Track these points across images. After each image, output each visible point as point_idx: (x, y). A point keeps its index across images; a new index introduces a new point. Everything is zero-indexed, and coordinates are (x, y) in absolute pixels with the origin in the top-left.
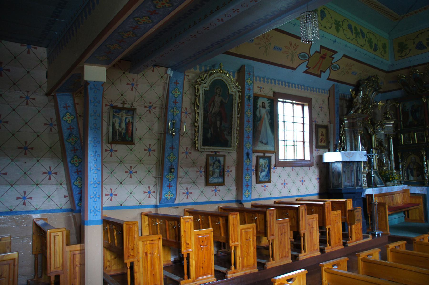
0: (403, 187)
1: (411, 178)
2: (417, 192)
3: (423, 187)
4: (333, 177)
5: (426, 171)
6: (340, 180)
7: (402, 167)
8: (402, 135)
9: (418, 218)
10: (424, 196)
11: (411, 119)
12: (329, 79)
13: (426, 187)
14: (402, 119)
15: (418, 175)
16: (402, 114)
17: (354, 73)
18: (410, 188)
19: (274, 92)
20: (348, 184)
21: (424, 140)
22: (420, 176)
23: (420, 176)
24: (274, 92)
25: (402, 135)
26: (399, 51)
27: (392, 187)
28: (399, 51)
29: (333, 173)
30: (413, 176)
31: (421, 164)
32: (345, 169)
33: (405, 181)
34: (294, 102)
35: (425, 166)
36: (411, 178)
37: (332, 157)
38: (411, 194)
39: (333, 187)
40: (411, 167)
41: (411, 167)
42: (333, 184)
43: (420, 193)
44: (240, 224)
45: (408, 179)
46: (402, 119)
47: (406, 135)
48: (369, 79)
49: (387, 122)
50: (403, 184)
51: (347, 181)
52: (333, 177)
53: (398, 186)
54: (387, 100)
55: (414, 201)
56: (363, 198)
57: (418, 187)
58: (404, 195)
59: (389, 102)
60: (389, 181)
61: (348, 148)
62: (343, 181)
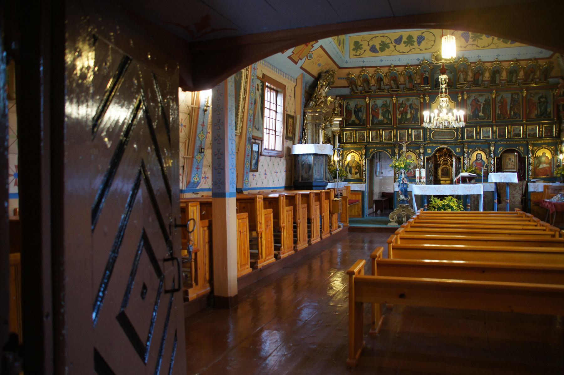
2: (356, 189)
4: (303, 169)
6: (311, 172)
9: (357, 214)
11: (353, 118)
12: (302, 68)
15: (356, 173)
17: (319, 65)
19: (263, 74)
20: (318, 177)
24: (263, 74)
26: (354, 50)
28: (354, 50)
29: (303, 165)
32: (315, 162)
34: (272, 87)
37: (299, 149)
39: (302, 180)
40: (350, 165)
42: (302, 176)
43: (359, 190)
44: (286, 206)
48: (327, 72)
50: (343, 182)
51: (317, 173)
52: (303, 169)
54: (336, 97)
55: (354, 198)
59: (338, 98)
61: (309, 141)
62: (314, 174)
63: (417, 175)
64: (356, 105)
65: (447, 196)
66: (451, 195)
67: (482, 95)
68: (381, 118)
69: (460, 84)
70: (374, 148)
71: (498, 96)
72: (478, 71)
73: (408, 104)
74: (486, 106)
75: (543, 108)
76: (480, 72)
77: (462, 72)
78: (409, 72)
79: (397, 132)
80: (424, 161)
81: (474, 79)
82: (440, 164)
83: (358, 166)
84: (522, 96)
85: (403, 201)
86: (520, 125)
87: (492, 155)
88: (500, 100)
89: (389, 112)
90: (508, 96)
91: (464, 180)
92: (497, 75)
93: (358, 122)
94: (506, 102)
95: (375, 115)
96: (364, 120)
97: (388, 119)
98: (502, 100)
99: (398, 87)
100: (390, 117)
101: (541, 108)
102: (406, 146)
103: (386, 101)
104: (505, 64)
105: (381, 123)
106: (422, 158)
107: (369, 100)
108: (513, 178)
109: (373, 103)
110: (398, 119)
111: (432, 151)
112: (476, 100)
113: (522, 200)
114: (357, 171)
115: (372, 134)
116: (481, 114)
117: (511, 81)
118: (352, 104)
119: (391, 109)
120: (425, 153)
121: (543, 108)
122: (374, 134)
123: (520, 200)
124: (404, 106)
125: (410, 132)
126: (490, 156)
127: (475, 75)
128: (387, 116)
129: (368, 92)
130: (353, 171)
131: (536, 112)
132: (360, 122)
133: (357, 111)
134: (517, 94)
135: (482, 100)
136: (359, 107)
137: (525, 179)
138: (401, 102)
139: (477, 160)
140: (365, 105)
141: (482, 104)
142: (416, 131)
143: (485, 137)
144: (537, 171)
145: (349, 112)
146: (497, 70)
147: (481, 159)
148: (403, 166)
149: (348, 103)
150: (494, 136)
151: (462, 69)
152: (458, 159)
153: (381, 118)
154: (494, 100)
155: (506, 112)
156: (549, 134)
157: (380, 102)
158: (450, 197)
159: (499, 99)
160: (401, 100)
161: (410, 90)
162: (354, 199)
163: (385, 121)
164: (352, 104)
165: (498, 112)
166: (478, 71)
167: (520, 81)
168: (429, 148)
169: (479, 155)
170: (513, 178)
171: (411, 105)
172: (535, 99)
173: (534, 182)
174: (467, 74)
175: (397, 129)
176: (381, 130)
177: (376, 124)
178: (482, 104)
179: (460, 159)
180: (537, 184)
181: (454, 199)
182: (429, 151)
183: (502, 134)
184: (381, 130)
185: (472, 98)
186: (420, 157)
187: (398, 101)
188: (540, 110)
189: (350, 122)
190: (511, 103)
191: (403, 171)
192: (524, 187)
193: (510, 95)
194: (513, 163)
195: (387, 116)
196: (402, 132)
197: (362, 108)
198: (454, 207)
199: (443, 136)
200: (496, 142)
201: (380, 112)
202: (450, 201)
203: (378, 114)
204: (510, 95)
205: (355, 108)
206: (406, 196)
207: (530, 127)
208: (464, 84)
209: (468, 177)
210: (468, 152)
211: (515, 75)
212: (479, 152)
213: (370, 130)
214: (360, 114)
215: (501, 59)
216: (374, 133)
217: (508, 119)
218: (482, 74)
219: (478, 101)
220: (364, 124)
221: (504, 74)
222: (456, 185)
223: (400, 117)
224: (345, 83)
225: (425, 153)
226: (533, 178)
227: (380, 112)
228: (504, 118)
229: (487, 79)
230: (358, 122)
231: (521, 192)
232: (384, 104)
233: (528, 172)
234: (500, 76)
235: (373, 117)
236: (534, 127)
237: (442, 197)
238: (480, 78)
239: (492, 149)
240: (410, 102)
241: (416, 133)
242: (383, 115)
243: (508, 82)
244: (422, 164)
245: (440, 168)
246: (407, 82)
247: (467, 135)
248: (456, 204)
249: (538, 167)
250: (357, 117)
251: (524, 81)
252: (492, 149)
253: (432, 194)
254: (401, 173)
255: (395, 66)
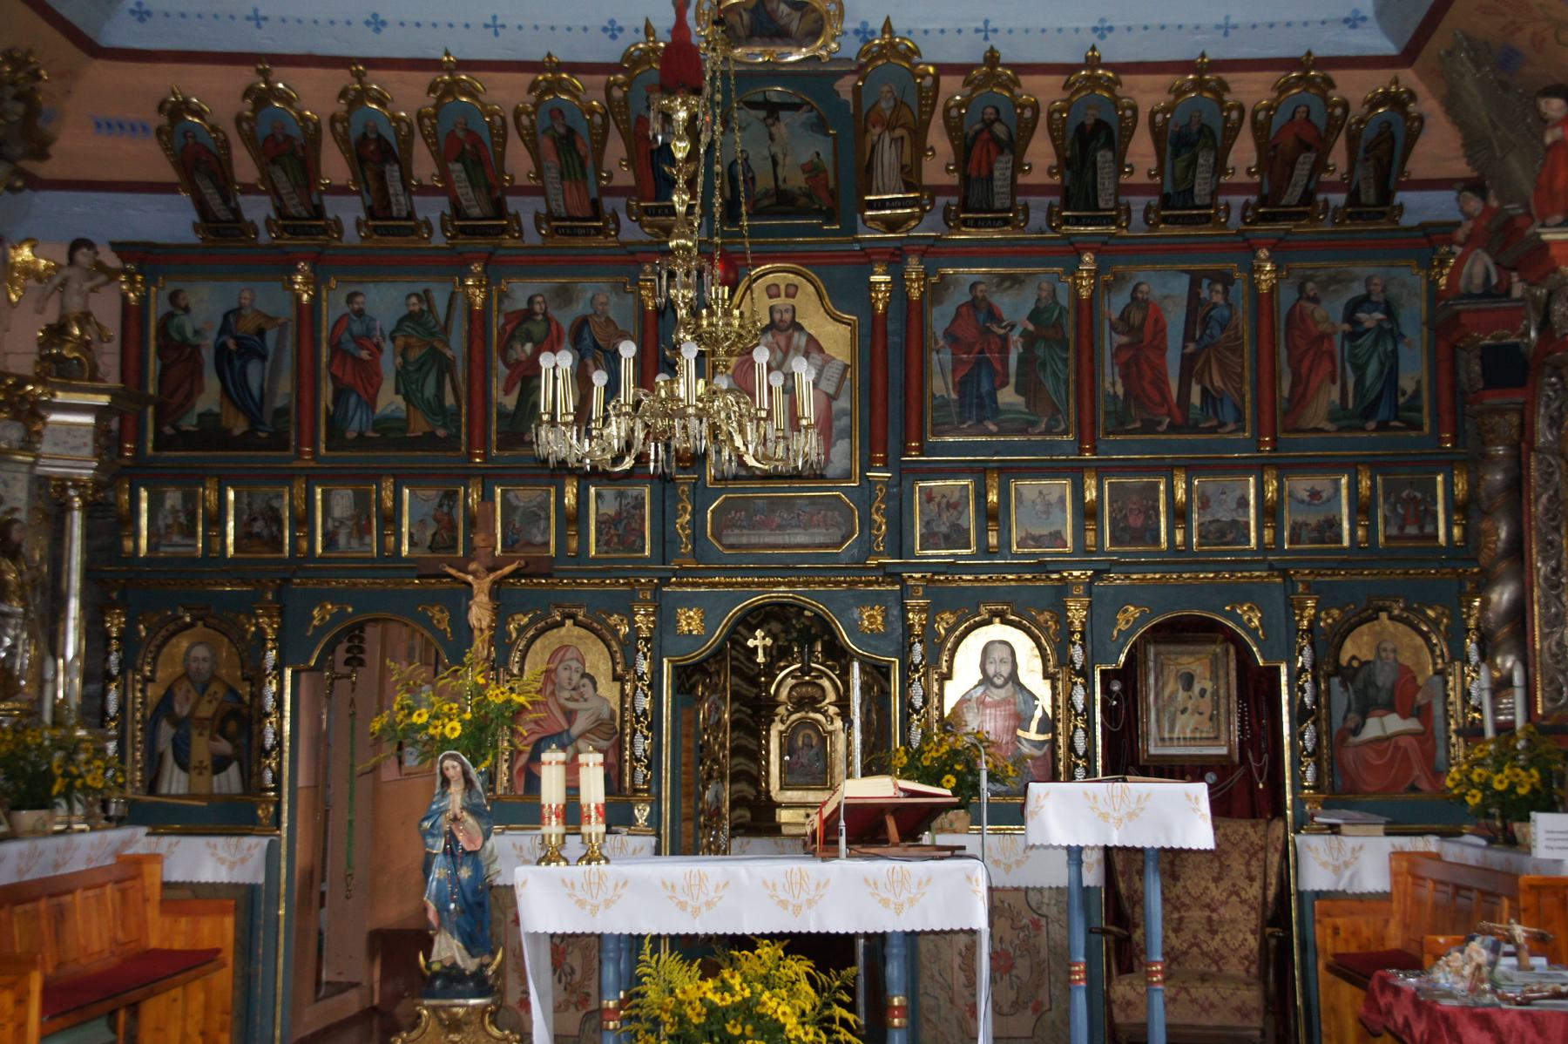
0: (126, 843)
1: (175, 782)
3: (248, 841)
5: (270, 740)
7: (122, 708)
8: (144, 494)
10: (244, 901)
11: (210, 397)
13: (265, 841)
14: (152, 390)
15: (220, 764)
16: (161, 354)
18: (164, 844)
21: (277, 543)
22: (233, 770)
23: (233, 770)
25: (144, 494)
27: (62, 840)
30: (184, 766)
31: (245, 690)
33: (131, 804)
35: (270, 704)
36: (175, 782)
38: (167, 886)
41: (181, 709)
45: (152, 786)
46: (152, 390)
47: (173, 498)
49: (61, 397)
50: (120, 822)
53: (95, 837)
56: (1221, 808)
57: (220, 841)
58: (123, 892)
60: (42, 802)
63: (552, 790)
64: (231, 318)
65: (746, 942)
66: (773, 937)
67: (1016, 281)
68: (389, 401)
69: (882, 205)
70: (333, 596)
71: (1108, 286)
72: (988, 125)
73: (565, 319)
74: (1040, 350)
75: (1372, 370)
76: (999, 130)
77: (890, 127)
78: (557, 112)
79: (487, 497)
80: (655, 686)
81: (965, 179)
82: (773, 703)
83: (233, 714)
84: (1254, 286)
85: (453, 979)
86: (1243, 468)
87: (1077, 653)
88: (1124, 316)
89: (446, 367)
90: (1169, 289)
91: (868, 830)
92: (1103, 157)
93: (239, 426)
94: (1160, 329)
95: (358, 380)
96: (282, 412)
97: (436, 409)
98: (1136, 317)
99: (499, 210)
100: (449, 400)
101: (1360, 370)
102: (495, 593)
103: (426, 297)
104: (1147, 95)
105: (390, 434)
106: (644, 666)
107: (315, 282)
108: (1182, 816)
109: (343, 308)
110: (502, 415)
111: (709, 626)
112: (980, 308)
113: (1264, 944)
114: (225, 747)
115: (331, 505)
116: (1008, 396)
117: (1185, 196)
118: (207, 305)
119: (456, 347)
120: (660, 639)
121: (1372, 370)
122: (343, 500)
123: (1253, 943)
124: (538, 330)
125: (570, 499)
126: (1065, 661)
127: (964, 151)
128: (430, 390)
129: (310, 232)
130: (202, 747)
131: (1335, 393)
132: (255, 421)
133: (240, 347)
134: (1226, 280)
135: (1015, 307)
136: (247, 326)
137: (1279, 811)
138: (523, 305)
139: (987, 680)
140: (287, 312)
141: (1015, 336)
142: (609, 492)
143: (1038, 541)
144: (1349, 756)
145: (179, 355)
146: (1100, 125)
147: (1013, 677)
148: (454, 729)
149: (174, 297)
150: (1090, 538)
151: (886, 106)
152: (877, 674)
153: (389, 401)
154: (1086, 311)
155: (1161, 383)
156: (1411, 530)
157: (385, 301)
158: (766, 951)
159: (1117, 303)
160: (521, 291)
161: (572, 232)
162: (179, 944)
163: (420, 426)
164: (207, 305)
165: (1112, 383)
166: (988, 125)
167: (1237, 200)
168: (689, 601)
169: (999, 653)
170: (1182, 816)
171: (581, 324)
172: (1330, 312)
173: (1334, 829)
174: (920, 149)
175: (488, 479)
176: (388, 484)
177: (361, 441)
178: (1015, 336)
179: (883, 672)
180: (1349, 842)
181: (799, 967)
182: (690, 621)
183: (1136, 521)
184: (388, 484)
185: (960, 296)
186: (631, 665)
187: (503, 296)
188: (1360, 381)
189: (189, 423)
190: (1188, 336)
191: (453, 768)
192: (1274, 859)
193: (1181, 286)
194: (1206, 705)
195: (430, 390)
196: (525, 496)
197: (271, 337)
198: (791, 1023)
199: (781, 527)
200: (1098, 574)
201: (388, 363)
202: (768, 982)
203: (370, 376)
204: (1185, 280)
205: (222, 331)
206: (472, 944)
207: (1301, 485)
208: (902, 203)
209: (896, 809)
210: (928, 628)
211: (1205, 160)
212: (997, 631)
213: (312, 478)
214: (254, 373)
215: (1114, 51)
216: (343, 500)
217: (1173, 428)
218: (1015, 146)
219: (993, 315)
220: (279, 442)
221: (1142, 152)
222: (813, 868)
223: (510, 402)
224: (154, 162)
225: (660, 639)
226: (1328, 805)
227: (388, 363)
228: (1149, 427)
229: (1038, 177)
230: (239, 426)
231: (1253, 891)
232: (413, 320)
233: (1297, 763)
234: (1120, 165)
235: (340, 395)
236: (1321, 483)
237: (709, 952)
238: (1002, 168)
239: (1077, 613)
240: (580, 308)
241: (610, 508)
242: (405, 385)
243: (1166, 202)
244: (644, 703)
245: (776, 728)
246: (552, 174)
247: (927, 524)
248: (807, 996)
249: (1356, 731)
250: (235, 391)
251: (1263, 201)
252: (1077, 613)
253: (648, 927)
254: (446, 782)
255: (465, 65)
